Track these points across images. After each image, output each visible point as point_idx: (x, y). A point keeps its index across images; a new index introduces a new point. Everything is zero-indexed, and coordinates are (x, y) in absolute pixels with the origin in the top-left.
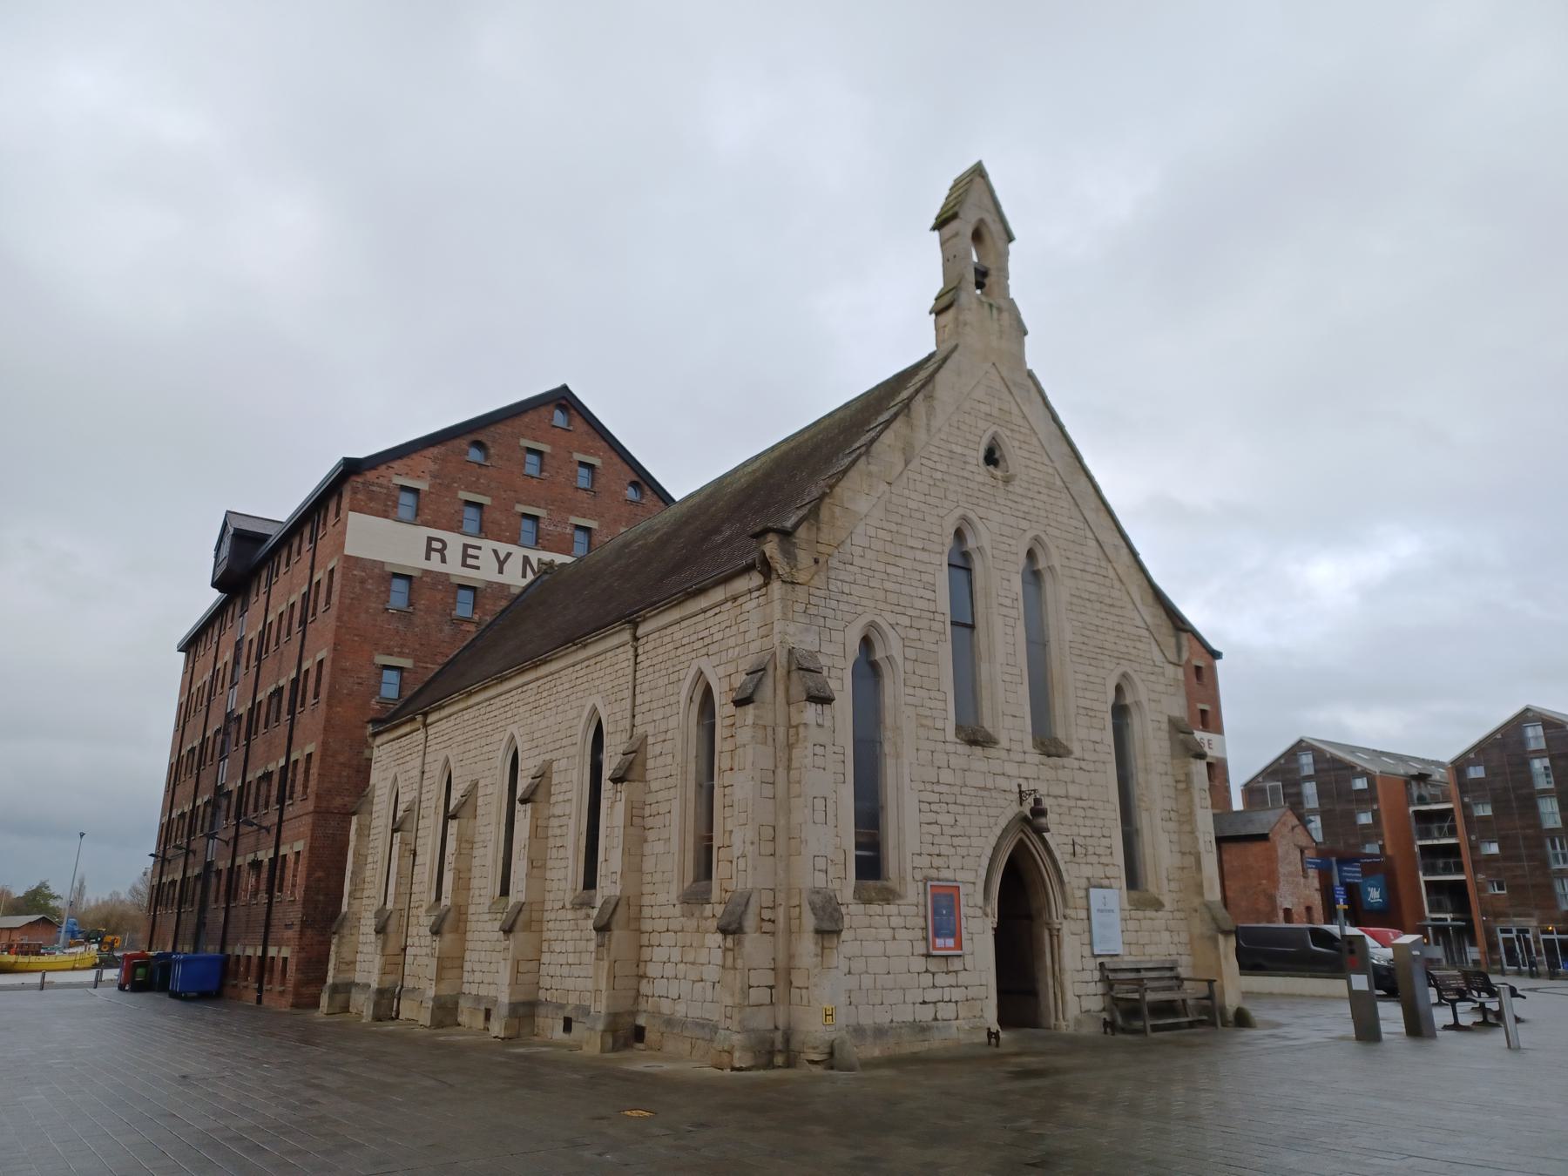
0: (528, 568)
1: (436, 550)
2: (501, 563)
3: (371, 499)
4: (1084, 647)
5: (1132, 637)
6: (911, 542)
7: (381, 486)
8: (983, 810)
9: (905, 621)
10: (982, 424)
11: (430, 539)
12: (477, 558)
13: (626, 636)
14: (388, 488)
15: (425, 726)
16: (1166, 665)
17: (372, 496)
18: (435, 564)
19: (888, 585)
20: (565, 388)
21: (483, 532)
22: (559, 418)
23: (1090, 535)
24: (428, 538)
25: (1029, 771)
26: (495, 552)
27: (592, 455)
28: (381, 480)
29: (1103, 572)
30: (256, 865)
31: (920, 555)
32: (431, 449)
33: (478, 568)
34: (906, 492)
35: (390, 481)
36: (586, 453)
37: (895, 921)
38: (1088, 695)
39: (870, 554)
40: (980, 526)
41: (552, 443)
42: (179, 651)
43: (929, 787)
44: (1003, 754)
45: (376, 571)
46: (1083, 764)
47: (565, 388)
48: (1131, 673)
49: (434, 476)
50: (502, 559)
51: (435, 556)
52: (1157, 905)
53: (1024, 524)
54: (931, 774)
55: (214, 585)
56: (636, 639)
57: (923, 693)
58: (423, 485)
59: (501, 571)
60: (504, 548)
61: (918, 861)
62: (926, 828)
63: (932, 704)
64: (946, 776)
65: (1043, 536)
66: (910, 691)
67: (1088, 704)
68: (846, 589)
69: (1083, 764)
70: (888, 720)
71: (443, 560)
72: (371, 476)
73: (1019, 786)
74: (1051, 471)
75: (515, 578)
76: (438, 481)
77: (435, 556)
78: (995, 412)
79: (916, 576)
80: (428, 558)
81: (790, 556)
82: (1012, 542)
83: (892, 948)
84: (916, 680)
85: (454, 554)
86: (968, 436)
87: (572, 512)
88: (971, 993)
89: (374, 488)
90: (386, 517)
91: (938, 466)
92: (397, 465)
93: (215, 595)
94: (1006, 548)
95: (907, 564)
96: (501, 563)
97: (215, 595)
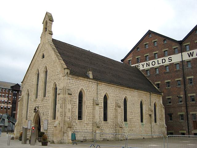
2: (143, 66)
20: (149, 30)
26: (142, 64)
36: (154, 40)
47: (149, 30)
60: (143, 63)
87: (153, 51)
92: (128, 57)
96: (143, 66)
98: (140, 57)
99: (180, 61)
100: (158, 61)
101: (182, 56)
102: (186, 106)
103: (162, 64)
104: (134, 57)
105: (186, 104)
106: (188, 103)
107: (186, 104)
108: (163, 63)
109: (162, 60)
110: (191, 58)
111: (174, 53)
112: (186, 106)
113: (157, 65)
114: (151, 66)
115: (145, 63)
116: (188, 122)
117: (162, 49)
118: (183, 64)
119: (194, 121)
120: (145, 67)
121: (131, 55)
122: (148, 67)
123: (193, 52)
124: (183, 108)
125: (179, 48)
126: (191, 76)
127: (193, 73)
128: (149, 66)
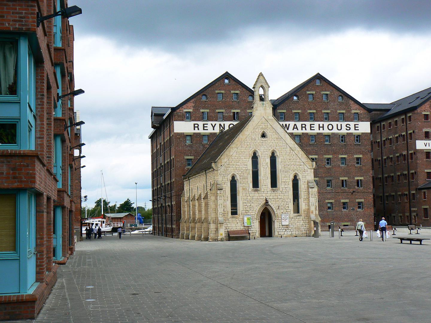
2: (214, 127)
5: (298, 165)
7: (180, 113)
8: (257, 203)
9: (241, 172)
10: (260, 130)
11: (194, 124)
12: (207, 127)
13: (204, 173)
15: (189, 180)
16: (308, 169)
17: (179, 116)
18: (196, 131)
20: (227, 72)
21: (209, 120)
22: (226, 81)
23: (288, 146)
24: (194, 124)
25: (267, 195)
26: (212, 124)
28: (181, 111)
29: (291, 153)
30: (169, 205)
32: (192, 100)
34: (241, 149)
36: (235, 90)
37: (237, 221)
38: (284, 179)
39: (233, 162)
40: (259, 151)
41: (225, 90)
42: (149, 138)
43: (245, 200)
44: (262, 192)
45: (182, 135)
46: (282, 192)
47: (227, 72)
48: (298, 173)
49: (194, 107)
51: (196, 129)
55: (152, 127)
56: (206, 173)
58: (191, 110)
59: (214, 129)
60: (213, 123)
61: (242, 212)
62: (244, 207)
63: (246, 186)
64: (249, 198)
66: (241, 184)
67: (285, 181)
69: (282, 192)
70: (237, 190)
71: (198, 129)
72: (178, 111)
73: (266, 198)
74: (278, 135)
75: (217, 130)
76: (195, 108)
77: (196, 129)
78: (264, 127)
80: (194, 129)
81: (216, 166)
83: (237, 225)
84: (243, 182)
85: (201, 127)
86: (256, 134)
90: (183, 121)
92: (184, 106)
93: (152, 130)
95: (241, 162)
96: (214, 127)
97: (152, 130)
98: (208, 111)
104: (196, 108)
117: (245, 109)
121: (191, 104)
123: (289, 125)
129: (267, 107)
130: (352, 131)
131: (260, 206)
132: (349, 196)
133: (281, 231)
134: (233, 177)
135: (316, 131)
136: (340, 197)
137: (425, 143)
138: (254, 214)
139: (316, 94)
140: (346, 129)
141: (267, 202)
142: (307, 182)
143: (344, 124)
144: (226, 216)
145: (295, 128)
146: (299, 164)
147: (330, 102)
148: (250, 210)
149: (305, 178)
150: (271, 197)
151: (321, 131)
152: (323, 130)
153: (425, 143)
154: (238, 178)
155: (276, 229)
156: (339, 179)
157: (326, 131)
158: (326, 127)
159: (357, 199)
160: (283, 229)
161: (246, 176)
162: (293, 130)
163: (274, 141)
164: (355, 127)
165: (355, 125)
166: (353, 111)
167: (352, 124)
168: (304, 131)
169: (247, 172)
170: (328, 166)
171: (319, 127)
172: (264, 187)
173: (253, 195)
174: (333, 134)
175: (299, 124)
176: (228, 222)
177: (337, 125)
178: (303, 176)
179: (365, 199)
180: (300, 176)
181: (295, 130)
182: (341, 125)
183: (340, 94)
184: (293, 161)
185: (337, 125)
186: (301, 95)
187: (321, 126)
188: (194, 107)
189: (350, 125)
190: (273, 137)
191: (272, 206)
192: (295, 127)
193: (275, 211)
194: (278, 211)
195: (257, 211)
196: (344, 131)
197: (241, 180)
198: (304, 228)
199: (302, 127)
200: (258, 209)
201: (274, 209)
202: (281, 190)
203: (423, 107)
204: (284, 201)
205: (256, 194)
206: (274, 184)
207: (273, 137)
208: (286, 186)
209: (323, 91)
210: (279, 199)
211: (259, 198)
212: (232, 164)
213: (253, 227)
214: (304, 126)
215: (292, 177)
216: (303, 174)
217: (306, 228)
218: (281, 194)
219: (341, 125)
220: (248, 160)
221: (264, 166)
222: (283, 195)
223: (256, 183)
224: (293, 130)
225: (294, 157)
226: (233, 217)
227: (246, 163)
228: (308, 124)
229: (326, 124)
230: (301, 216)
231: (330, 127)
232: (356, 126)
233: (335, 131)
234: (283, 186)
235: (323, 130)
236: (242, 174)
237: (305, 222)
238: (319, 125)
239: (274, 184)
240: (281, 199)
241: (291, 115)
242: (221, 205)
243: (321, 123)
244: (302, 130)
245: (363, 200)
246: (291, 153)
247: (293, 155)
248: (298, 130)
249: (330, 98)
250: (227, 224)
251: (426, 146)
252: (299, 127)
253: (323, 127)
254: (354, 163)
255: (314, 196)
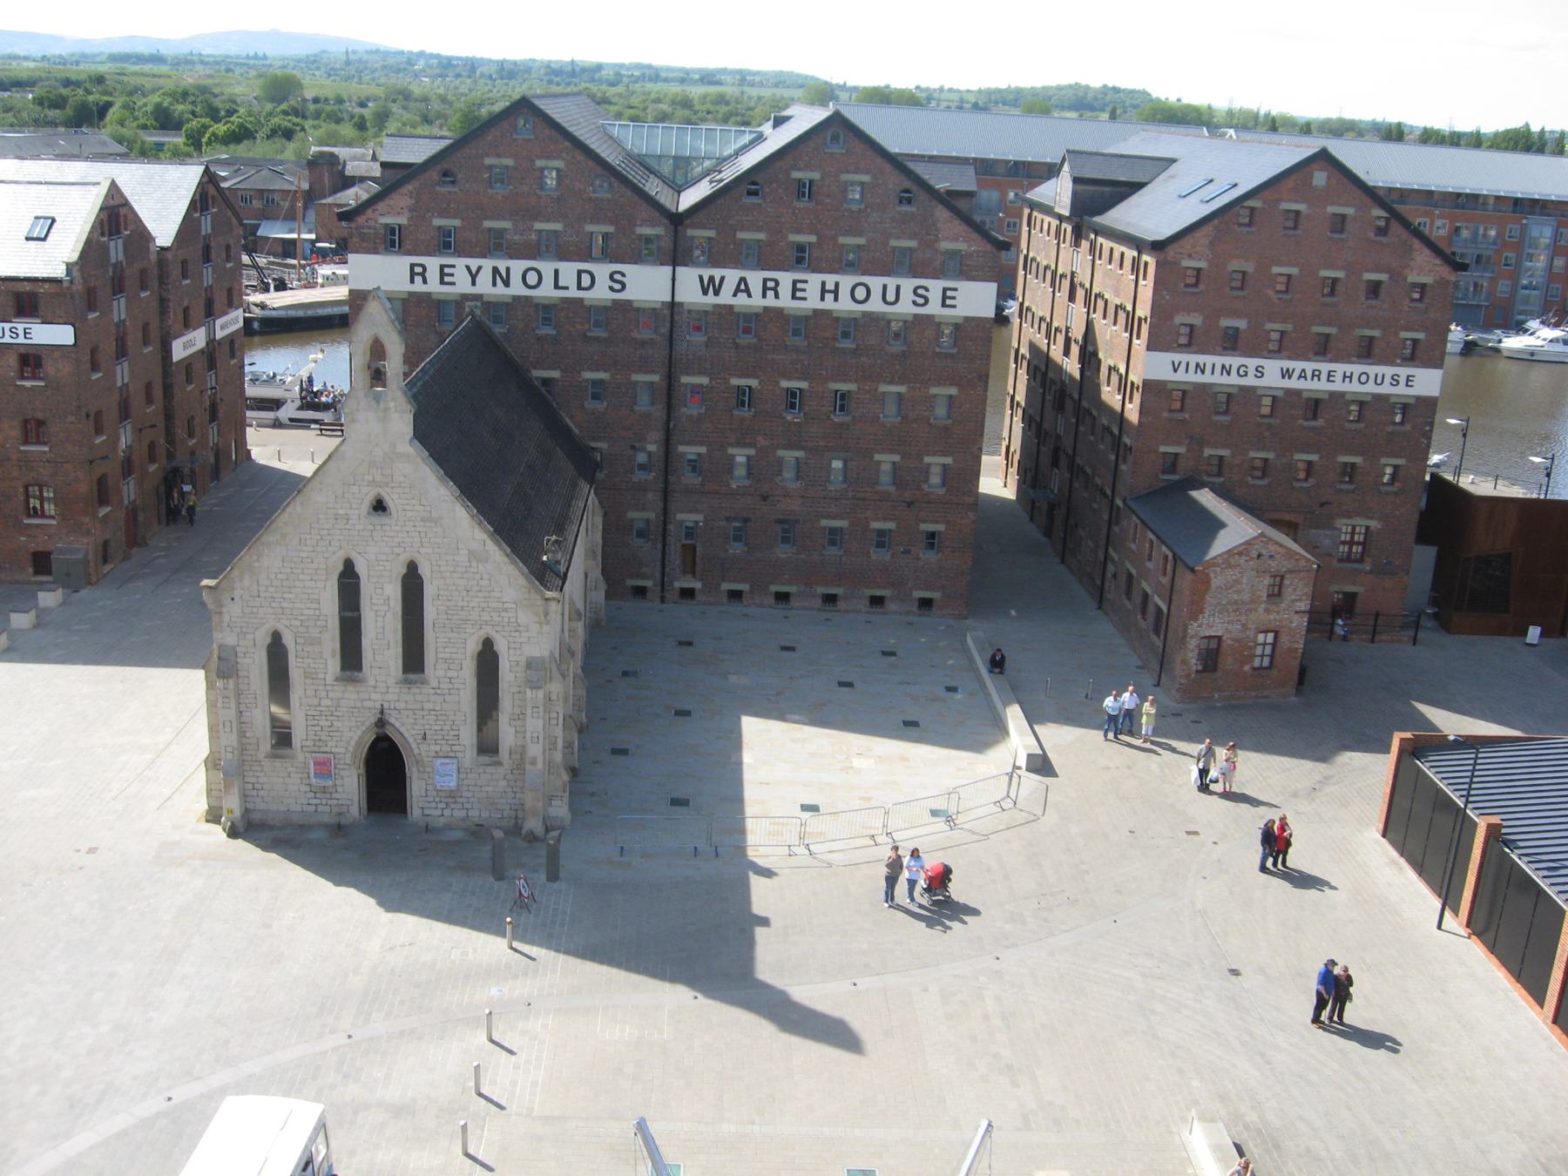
0: (504, 276)
1: (418, 274)
3: (363, 241)
4: (447, 622)
6: (302, 577)
7: (369, 228)
8: (353, 719)
10: (365, 490)
11: (412, 266)
12: (452, 275)
14: (375, 229)
17: (363, 238)
18: (418, 287)
19: (283, 605)
25: (388, 697)
26: (468, 268)
27: (555, 158)
28: (372, 223)
29: (472, 570)
31: (308, 584)
33: (454, 284)
34: (299, 547)
35: (376, 222)
36: (548, 158)
37: (290, 769)
39: (271, 589)
46: (438, 691)
49: (411, 210)
50: (474, 272)
51: (418, 279)
52: (500, 764)
53: (397, 550)
54: (316, 702)
57: (310, 661)
59: (474, 283)
60: (474, 263)
64: (326, 702)
65: (416, 555)
67: (448, 656)
68: (255, 610)
69: (438, 691)
71: (425, 281)
72: (361, 220)
77: (418, 279)
79: (305, 596)
80: (412, 281)
82: (385, 563)
83: (287, 780)
85: (433, 274)
87: (539, 216)
88: (340, 802)
89: (365, 231)
91: (326, 526)
92: (381, 206)
94: (381, 568)
99: (663, 302)
100: (556, 272)
101: (674, 280)
102: (666, 488)
103: (573, 293)
104: (419, 213)
105: (666, 482)
106: (672, 479)
107: (666, 482)
108: (580, 287)
109: (580, 273)
110: (711, 299)
111: (636, 259)
112: (666, 488)
113: (547, 291)
114: (517, 289)
115: (487, 264)
116: (664, 547)
118: (676, 317)
119: (684, 545)
120: (484, 286)
122: (500, 289)
123: (722, 279)
124: (652, 497)
125: (667, 243)
126: (700, 374)
127: (708, 366)
128: (507, 283)
129: (393, 410)
130: (934, 308)
131: (364, 728)
132: (897, 513)
133: (433, 805)
134: (276, 637)
135: (812, 301)
136: (868, 512)
137: (1173, 363)
138: (343, 750)
139: (822, 178)
140: (914, 303)
141: (381, 723)
142: (523, 664)
143: (908, 285)
144: (253, 753)
145: (742, 291)
146: (500, 605)
147: (869, 210)
148: (330, 738)
149: (518, 652)
150: (401, 705)
151: (829, 304)
152: (836, 299)
153: (1173, 363)
154: (288, 640)
155: (414, 799)
156: (872, 457)
157: (845, 305)
158: (844, 292)
159: (924, 522)
160: (437, 799)
161: (318, 635)
162: (735, 295)
163: (413, 529)
164: (944, 297)
165: (945, 290)
166: (945, 245)
167: (935, 287)
168: (770, 301)
169: (319, 623)
170: (838, 418)
171: (824, 291)
172: (376, 671)
173: (339, 695)
174: (865, 314)
175: (755, 278)
176: (259, 768)
177: (885, 287)
178: (512, 645)
179: (948, 523)
180: (501, 646)
181: (742, 297)
182: (898, 288)
183: (907, 184)
184: (479, 594)
185: (885, 287)
186: (771, 183)
187: (830, 286)
188: (411, 210)
189: (927, 290)
190: (409, 514)
191: (402, 730)
192: (743, 287)
193: (414, 746)
194: (424, 748)
195: (353, 743)
196: (906, 307)
197: (299, 648)
198: (509, 801)
199: (765, 289)
200: (356, 738)
201: (411, 740)
202: (434, 683)
203: (1186, 244)
204: (444, 718)
205: (350, 694)
206: (413, 659)
207: (409, 514)
208: (450, 674)
209: (848, 172)
210: (426, 713)
211: (358, 705)
212: (267, 594)
213: (339, 789)
214: (771, 284)
215: (473, 646)
216: (511, 639)
217: (515, 801)
218: (433, 698)
219: (898, 288)
220: (320, 585)
221: (375, 608)
222: (440, 699)
223: (351, 656)
224: (735, 295)
225: (481, 583)
226: (276, 756)
227: (316, 597)
228: (786, 279)
229: (846, 282)
230: (500, 764)
231: (860, 293)
232: (949, 293)
233: (875, 305)
234: (442, 673)
235: (836, 299)
236: (301, 629)
237: (512, 783)
238: (823, 284)
239: (413, 659)
240: (433, 713)
241: (732, 246)
242: (228, 724)
243: (831, 280)
244: (764, 296)
245: (940, 527)
246: (472, 570)
247: (478, 576)
248: (749, 295)
249: (869, 195)
250: (256, 774)
251: (1175, 370)
252: (756, 288)
253: (836, 292)
254: (927, 413)
255: (542, 713)
